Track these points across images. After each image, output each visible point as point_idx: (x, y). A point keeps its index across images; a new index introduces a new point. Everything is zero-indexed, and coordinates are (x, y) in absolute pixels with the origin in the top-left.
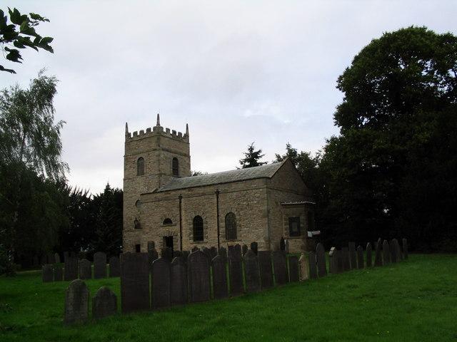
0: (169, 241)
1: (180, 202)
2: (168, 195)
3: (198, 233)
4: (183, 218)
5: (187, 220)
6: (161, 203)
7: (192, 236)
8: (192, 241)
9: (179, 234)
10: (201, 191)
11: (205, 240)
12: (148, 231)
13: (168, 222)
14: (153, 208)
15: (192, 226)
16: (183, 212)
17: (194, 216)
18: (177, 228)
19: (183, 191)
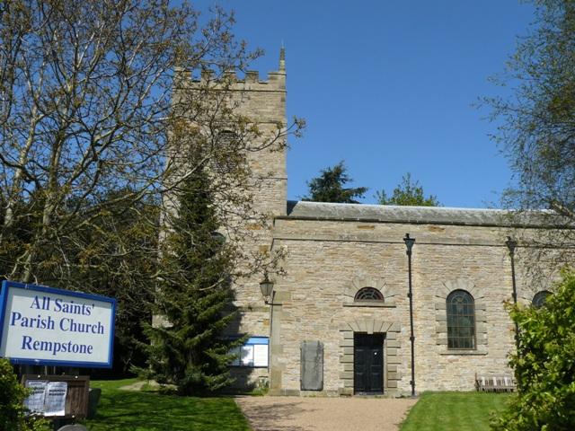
0: (369, 347)
1: (409, 253)
2: (368, 231)
3: (461, 335)
4: (416, 293)
5: (428, 298)
6: (346, 246)
7: (444, 336)
8: (444, 348)
9: (406, 330)
10: (466, 233)
11: (481, 348)
12: (300, 313)
13: (369, 295)
14: (319, 255)
15: (444, 313)
16: (416, 277)
17: (450, 288)
18: (400, 314)
19: (414, 230)
